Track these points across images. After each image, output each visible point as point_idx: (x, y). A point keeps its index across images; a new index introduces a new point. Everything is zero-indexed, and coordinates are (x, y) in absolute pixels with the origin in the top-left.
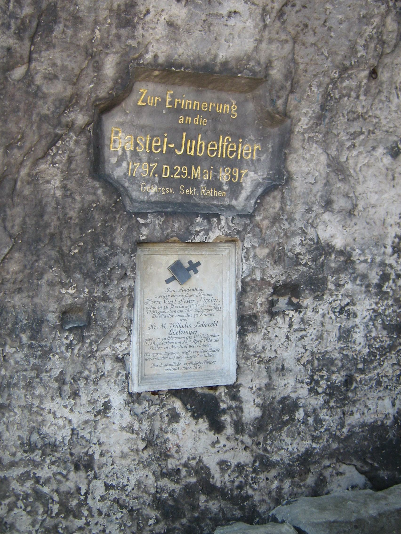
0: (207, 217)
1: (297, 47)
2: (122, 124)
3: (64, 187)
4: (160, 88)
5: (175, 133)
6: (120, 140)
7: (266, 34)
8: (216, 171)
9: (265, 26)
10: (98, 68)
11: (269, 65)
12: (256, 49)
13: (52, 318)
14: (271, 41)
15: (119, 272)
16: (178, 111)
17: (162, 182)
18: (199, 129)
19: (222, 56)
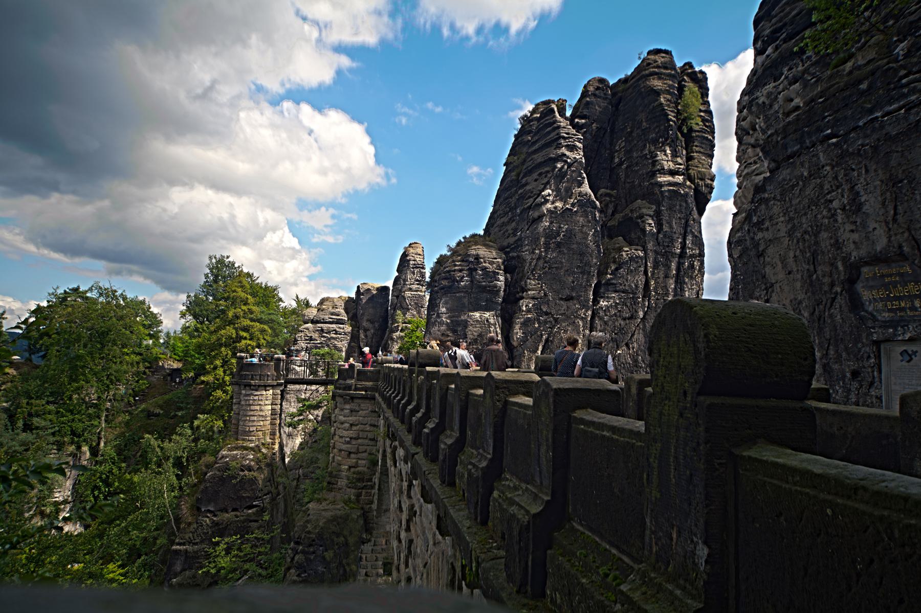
0: (902, 327)
1: (913, 232)
2: (863, 287)
3: (842, 319)
4: (872, 268)
5: (886, 286)
6: (866, 295)
7: (892, 233)
8: (913, 302)
9: (890, 229)
10: (837, 268)
11: (900, 247)
12: (889, 241)
13: (848, 375)
14: (896, 235)
15: (866, 355)
16: (883, 276)
17: (890, 311)
18: (896, 282)
19: (879, 249)
